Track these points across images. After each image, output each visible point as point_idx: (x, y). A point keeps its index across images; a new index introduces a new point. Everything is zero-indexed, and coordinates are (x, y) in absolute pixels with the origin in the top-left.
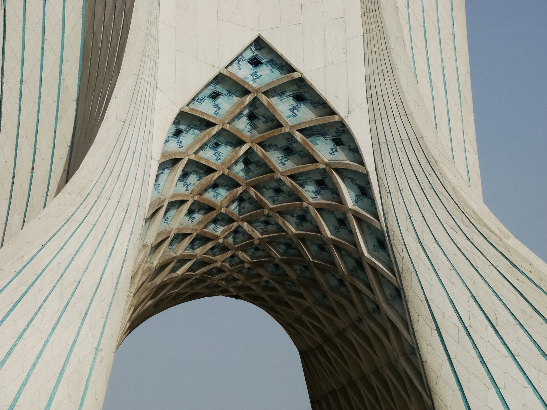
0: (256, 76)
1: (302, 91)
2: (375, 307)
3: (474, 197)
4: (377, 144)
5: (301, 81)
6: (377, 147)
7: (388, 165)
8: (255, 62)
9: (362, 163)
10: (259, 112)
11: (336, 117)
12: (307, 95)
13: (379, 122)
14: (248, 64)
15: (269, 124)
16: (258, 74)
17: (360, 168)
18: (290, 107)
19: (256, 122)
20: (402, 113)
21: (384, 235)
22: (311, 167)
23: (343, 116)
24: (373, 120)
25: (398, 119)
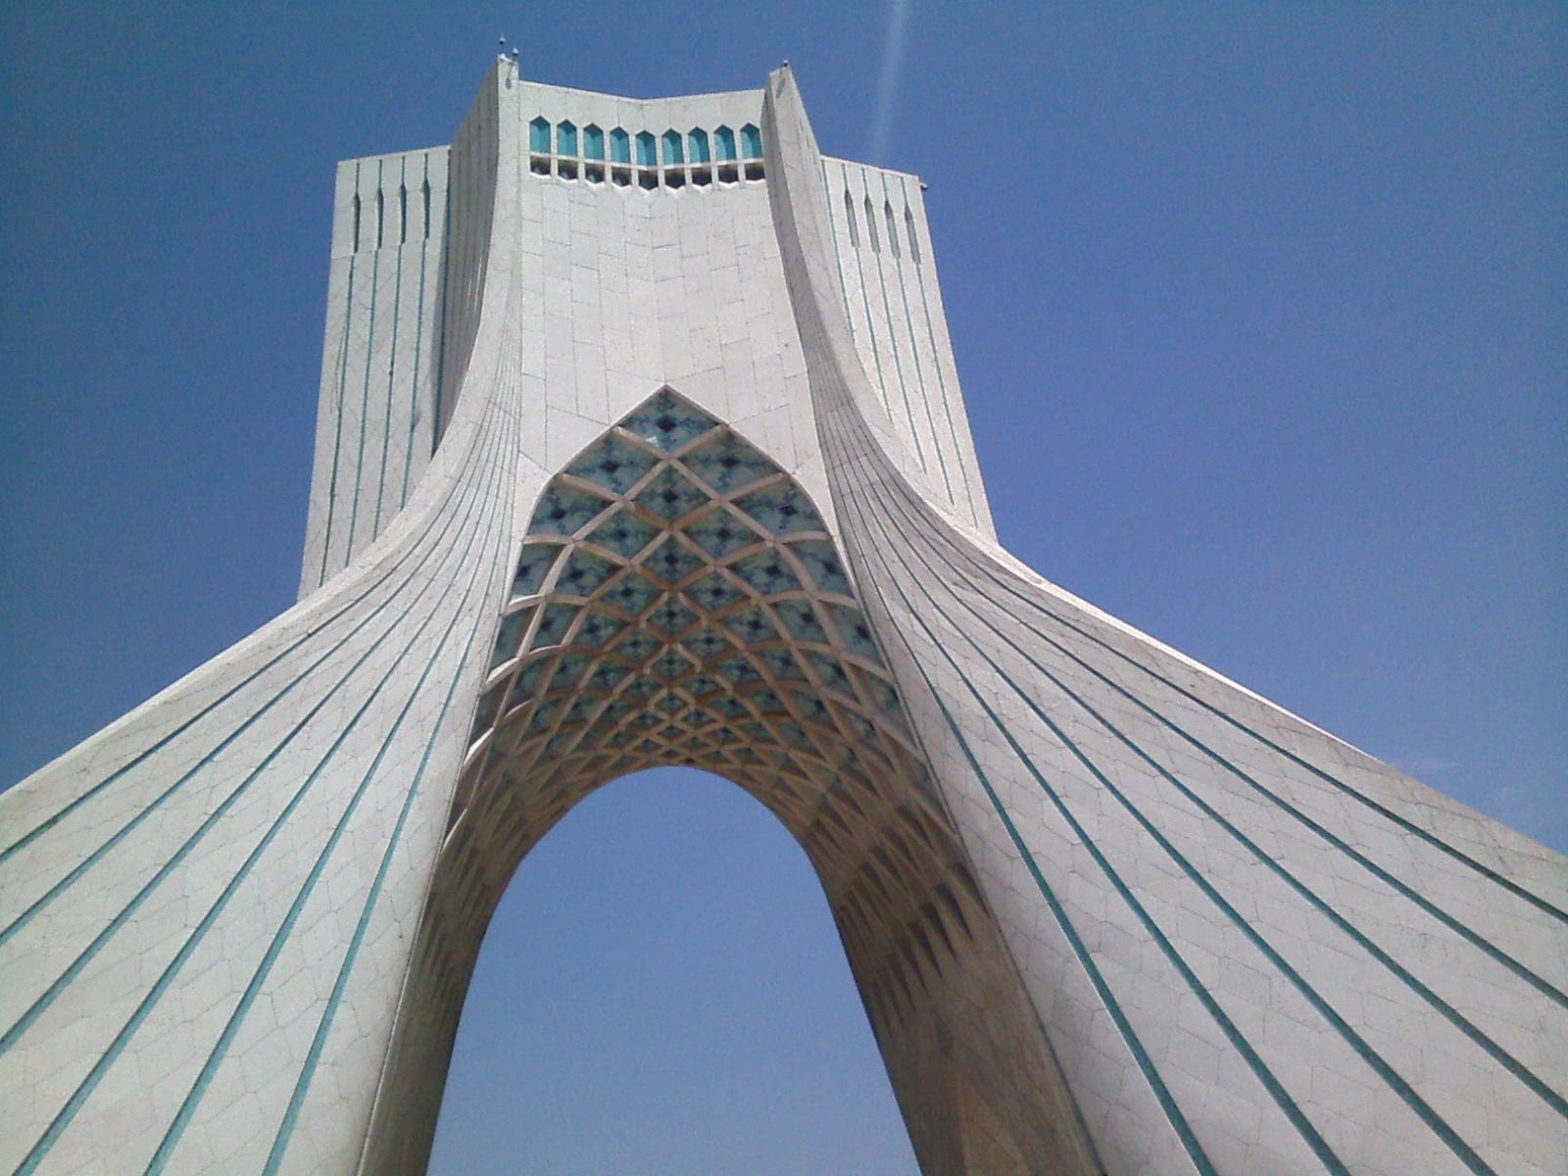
0: (667, 444)
1: (733, 454)
2: (868, 728)
3: (984, 539)
4: (837, 496)
5: (730, 438)
6: (840, 503)
7: (857, 522)
8: (667, 425)
9: (823, 529)
10: (680, 488)
11: (781, 474)
12: (740, 456)
13: (838, 471)
14: (657, 427)
15: (694, 503)
16: (672, 438)
17: (820, 536)
18: (719, 476)
19: (676, 503)
20: (868, 450)
21: (863, 620)
22: (753, 549)
23: (789, 471)
24: (831, 470)
25: (863, 459)
